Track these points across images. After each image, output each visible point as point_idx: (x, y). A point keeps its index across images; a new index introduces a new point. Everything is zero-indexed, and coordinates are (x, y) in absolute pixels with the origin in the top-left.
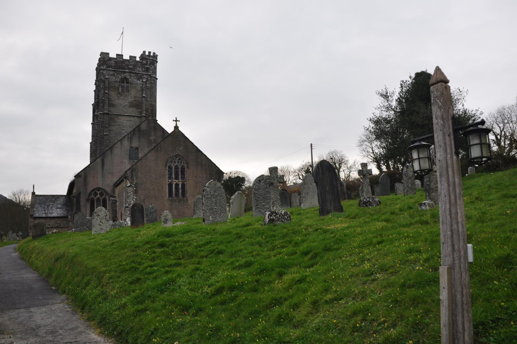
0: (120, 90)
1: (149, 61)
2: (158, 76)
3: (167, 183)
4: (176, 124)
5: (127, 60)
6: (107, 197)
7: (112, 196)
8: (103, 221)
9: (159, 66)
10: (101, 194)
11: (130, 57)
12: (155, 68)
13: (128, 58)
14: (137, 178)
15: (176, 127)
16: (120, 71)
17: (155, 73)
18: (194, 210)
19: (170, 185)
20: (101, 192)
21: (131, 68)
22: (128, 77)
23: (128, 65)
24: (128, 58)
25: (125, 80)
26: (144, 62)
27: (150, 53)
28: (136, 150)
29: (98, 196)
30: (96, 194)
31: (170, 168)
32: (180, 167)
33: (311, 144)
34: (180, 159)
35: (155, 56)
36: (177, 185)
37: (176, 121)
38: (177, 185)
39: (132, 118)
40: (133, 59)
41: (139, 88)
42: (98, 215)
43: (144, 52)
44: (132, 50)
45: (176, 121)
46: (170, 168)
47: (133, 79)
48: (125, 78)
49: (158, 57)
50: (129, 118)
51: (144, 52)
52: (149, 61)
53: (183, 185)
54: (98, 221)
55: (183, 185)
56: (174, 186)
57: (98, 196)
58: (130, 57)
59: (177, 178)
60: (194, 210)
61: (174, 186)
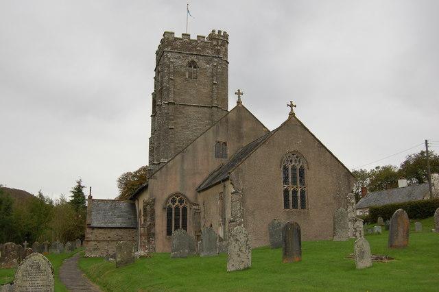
0: (187, 77)
1: (218, 42)
2: (231, 58)
3: (283, 189)
4: (292, 110)
5: (196, 41)
6: (188, 205)
7: (195, 205)
8: (243, 249)
9: (231, 48)
10: (181, 201)
11: (198, 36)
12: (226, 50)
13: (196, 38)
14: (244, 181)
15: (292, 115)
16: (187, 54)
17: (226, 56)
18: (335, 228)
19: (286, 192)
20: (181, 199)
21: (199, 50)
22: (196, 60)
23: (195, 47)
24: (196, 38)
25: (192, 64)
26: (215, 43)
27: (220, 32)
28: (224, 146)
29: (177, 203)
30: (173, 201)
31: (285, 169)
32: (290, 167)
33: (426, 141)
34: (297, 157)
35: (226, 36)
36: (295, 192)
37: (291, 106)
38: (295, 192)
39: (201, 109)
40: (202, 39)
41: (209, 74)
42: (237, 240)
43: (214, 31)
44: (198, 29)
45: (291, 106)
46: (285, 169)
47: (201, 63)
48: (193, 62)
49: (229, 38)
50: (198, 109)
51: (214, 31)
52: (218, 42)
53: (303, 192)
54: (237, 249)
55: (303, 192)
56: (291, 193)
57: (177, 203)
58: (198, 36)
59: (294, 183)
60: (335, 228)
61: (291, 193)
